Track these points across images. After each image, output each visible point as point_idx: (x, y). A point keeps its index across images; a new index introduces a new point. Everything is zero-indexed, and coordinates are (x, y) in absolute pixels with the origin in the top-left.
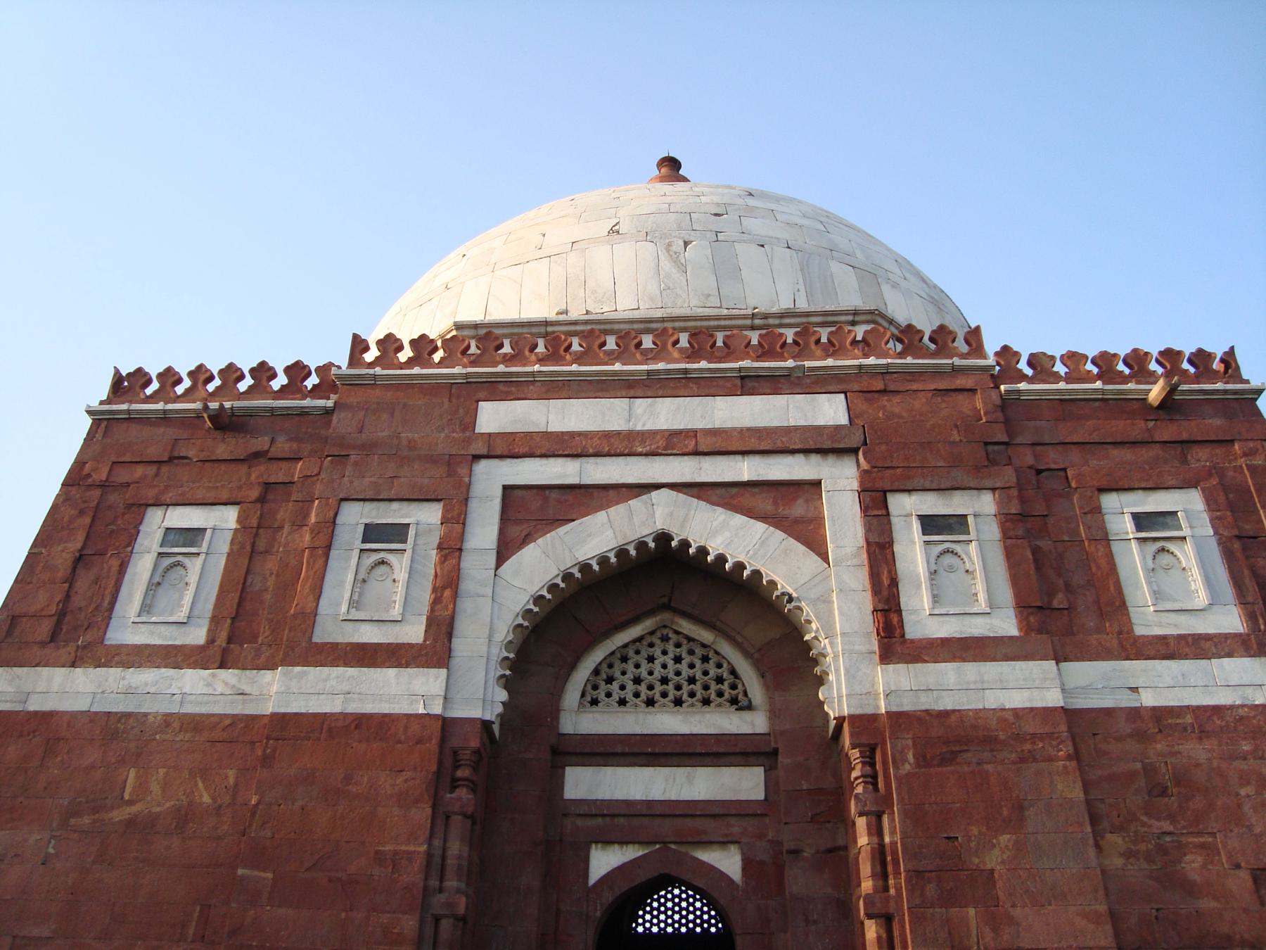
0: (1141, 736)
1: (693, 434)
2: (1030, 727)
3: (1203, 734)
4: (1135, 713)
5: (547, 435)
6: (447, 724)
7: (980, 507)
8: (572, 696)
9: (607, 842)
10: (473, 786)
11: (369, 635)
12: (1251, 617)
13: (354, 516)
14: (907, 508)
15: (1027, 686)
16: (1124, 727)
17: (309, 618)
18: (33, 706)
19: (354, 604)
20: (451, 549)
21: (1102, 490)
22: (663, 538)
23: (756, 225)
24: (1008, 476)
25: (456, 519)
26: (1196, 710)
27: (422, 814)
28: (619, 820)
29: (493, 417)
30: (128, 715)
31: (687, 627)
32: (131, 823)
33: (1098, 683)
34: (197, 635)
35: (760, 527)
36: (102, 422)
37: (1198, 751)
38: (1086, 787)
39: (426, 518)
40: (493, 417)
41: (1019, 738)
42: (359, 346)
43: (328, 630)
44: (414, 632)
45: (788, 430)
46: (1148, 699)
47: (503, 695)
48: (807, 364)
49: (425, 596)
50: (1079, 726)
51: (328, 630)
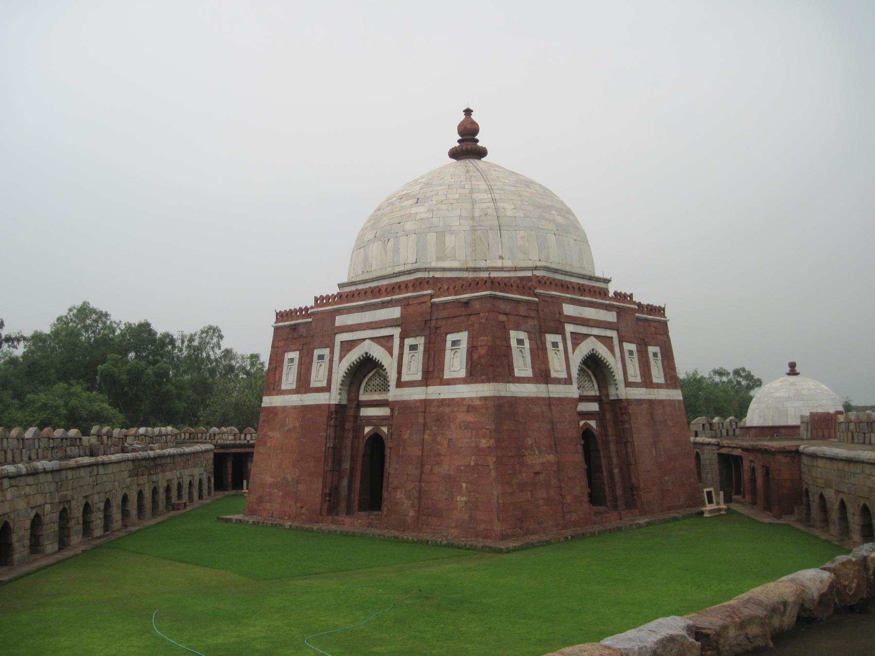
0: (438, 406)
1: (371, 323)
2: (418, 404)
3: (449, 405)
4: (438, 400)
5: (347, 326)
6: (329, 405)
7: (420, 341)
8: (362, 391)
9: (368, 425)
10: (336, 419)
11: (319, 385)
12: (467, 372)
13: (317, 352)
14: (408, 342)
15: (417, 394)
16: (435, 404)
17: (309, 382)
18: (274, 405)
19: (317, 377)
20: (331, 361)
21: (447, 334)
22: (366, 353)
23: (409, 226)
24: (427, 332)
25: (332, 352)
26: (449, 399)
27: (325, 427)
28: (369, 420)
29: (341, 320)
30: (285, 407)
31: (381, 371)
32: (288, 430)
33: (435, 392)
34: (294, 386)
35: (382, 349)
36: (277, 329)
37: (447, 410)
38: (425, 418)
39: (326, 352)
40: (340, 320)
41: (415, 407)
42: (316, 299)
43: (314, 384)
44: (324, 384)
45: (388, 320)
46: (442, 397)
47: (339, 397)
48: (395, 297)
49: (326, 374)
50: (426, 403)
51: (314, 384)
